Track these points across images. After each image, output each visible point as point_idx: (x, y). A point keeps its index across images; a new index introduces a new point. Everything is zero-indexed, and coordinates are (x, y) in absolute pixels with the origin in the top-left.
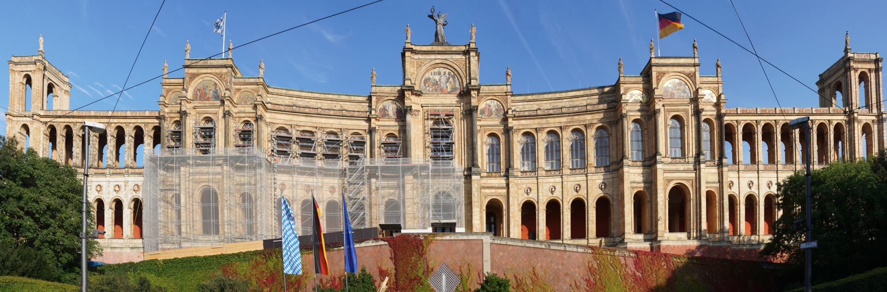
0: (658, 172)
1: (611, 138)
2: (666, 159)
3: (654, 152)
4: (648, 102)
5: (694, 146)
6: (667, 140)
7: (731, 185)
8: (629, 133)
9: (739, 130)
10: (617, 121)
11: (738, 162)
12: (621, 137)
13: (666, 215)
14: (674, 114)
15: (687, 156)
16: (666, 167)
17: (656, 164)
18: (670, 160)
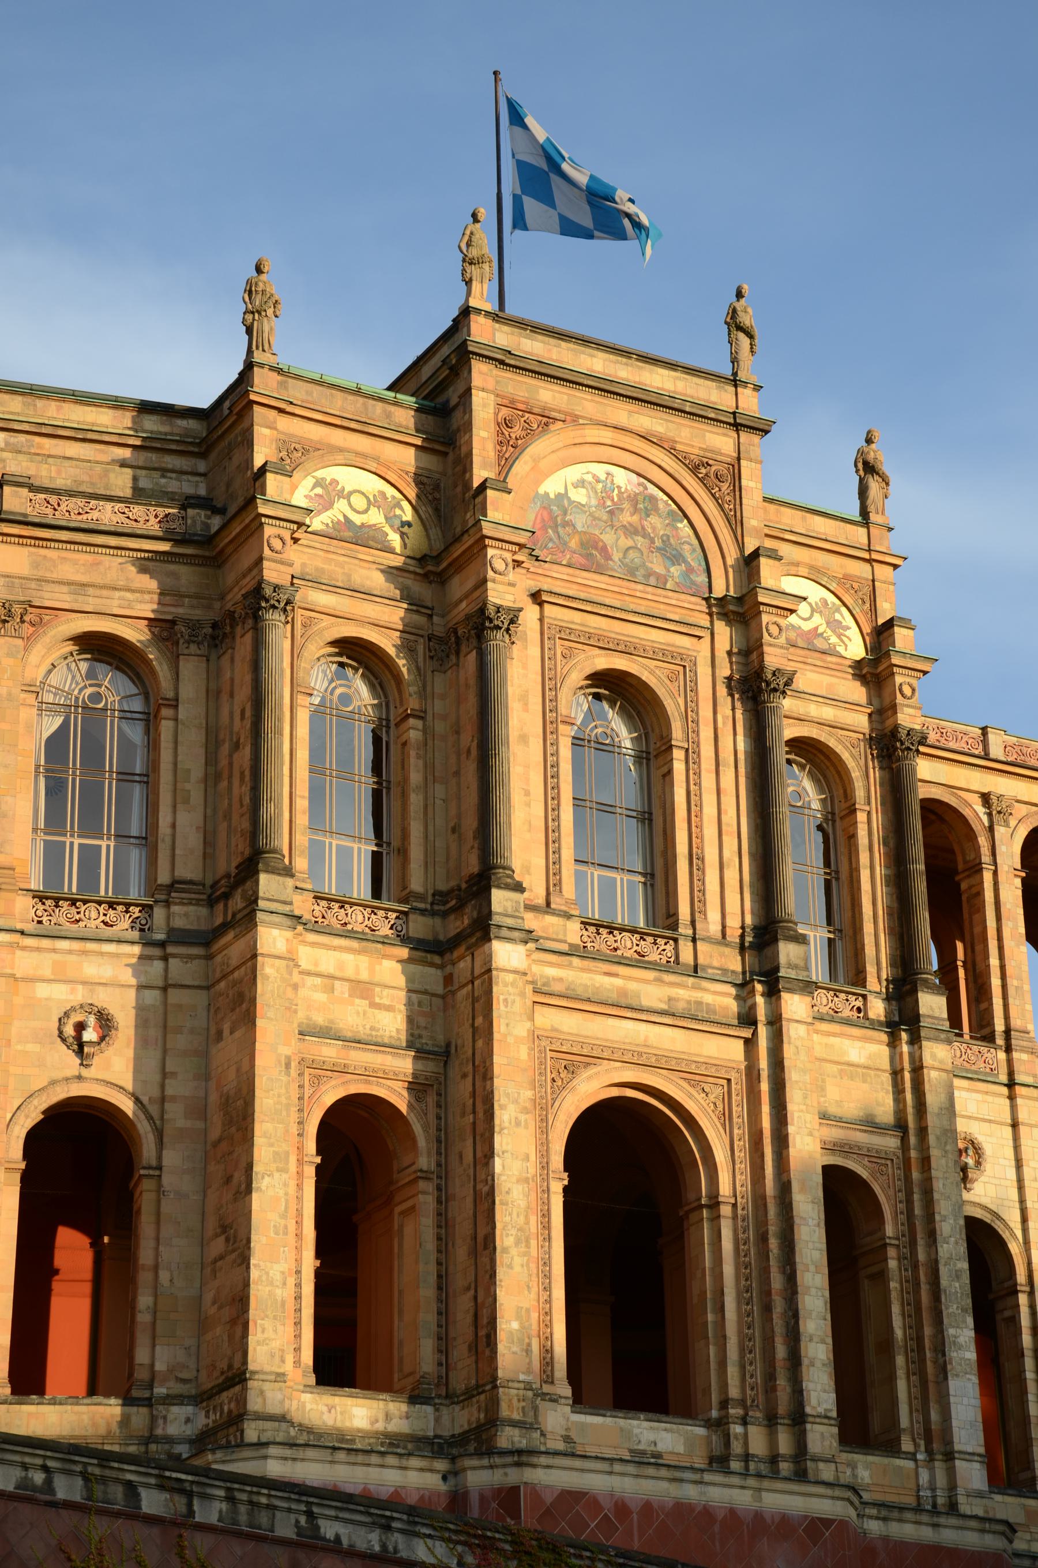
0: (499, 991)
1: (166, 728)
2: (550, 919)
3: (473, 865)
4: (438, 558)
5: (732, 876)
6: (557, 808)
7: (970, 1161)
8: (303, 717)
9: (1001, 849)
10: (215, 626)
11: (1008, 1032)
12: (242, 728)
13: (548, 1276)
14: (603, 662)
15: (685, 930)
16: (551, 972)
17: (487, 938)
18: (573, 932)
